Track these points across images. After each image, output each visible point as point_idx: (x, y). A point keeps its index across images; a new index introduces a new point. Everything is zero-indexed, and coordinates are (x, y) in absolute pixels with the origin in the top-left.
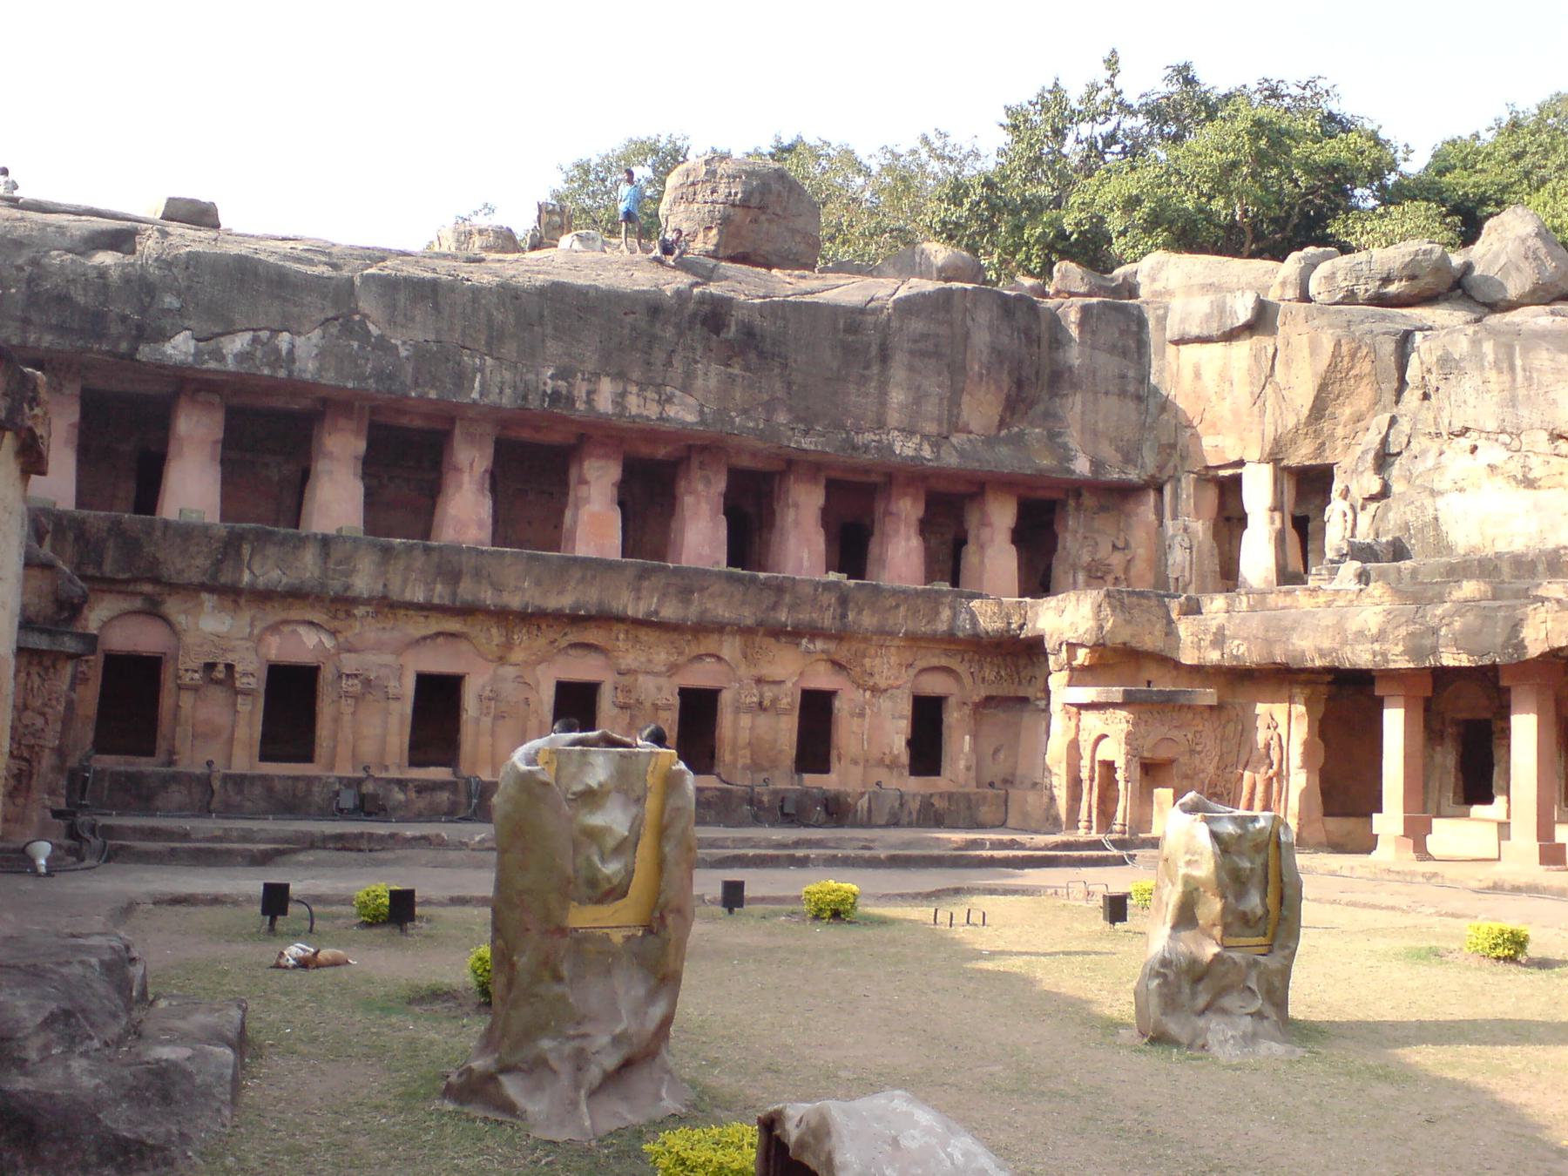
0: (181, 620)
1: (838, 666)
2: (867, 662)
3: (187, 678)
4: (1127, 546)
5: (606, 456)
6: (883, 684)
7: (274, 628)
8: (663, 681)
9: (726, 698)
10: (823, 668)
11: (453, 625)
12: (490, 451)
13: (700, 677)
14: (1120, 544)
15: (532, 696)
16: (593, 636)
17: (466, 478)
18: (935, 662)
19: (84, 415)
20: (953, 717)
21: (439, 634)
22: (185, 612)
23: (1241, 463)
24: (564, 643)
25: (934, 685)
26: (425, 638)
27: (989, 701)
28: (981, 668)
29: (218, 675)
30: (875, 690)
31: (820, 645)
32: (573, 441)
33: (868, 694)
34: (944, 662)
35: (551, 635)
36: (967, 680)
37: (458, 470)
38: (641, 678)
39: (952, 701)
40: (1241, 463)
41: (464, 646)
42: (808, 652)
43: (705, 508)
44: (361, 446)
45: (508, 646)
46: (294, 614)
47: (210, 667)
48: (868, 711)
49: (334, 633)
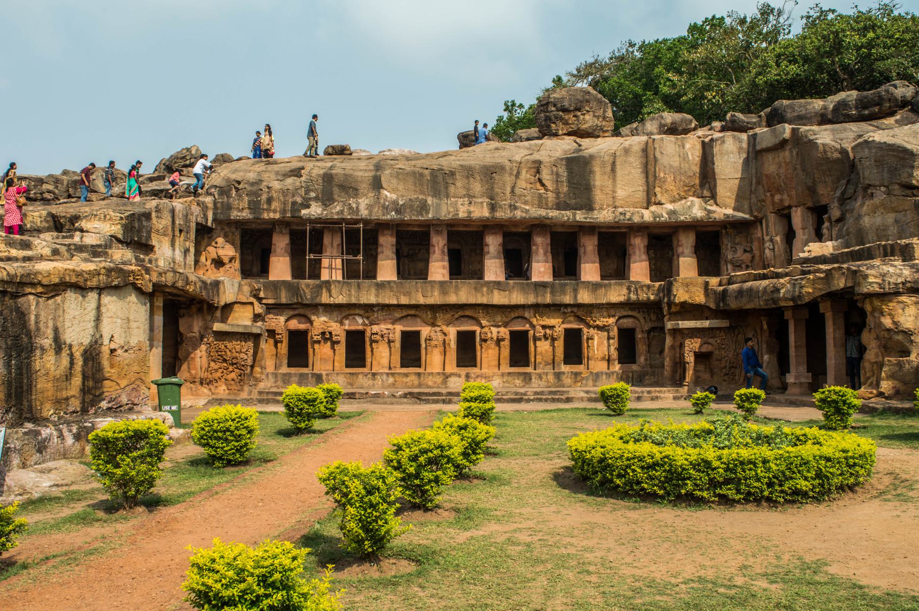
0: (313, 318)
1: (580, 320)
3: (315, 338)
4: (752, 250)
5: (495, 233)
7: (346, 317)
8: (502, 329)
10: (572, 319)
11: (412, 312)
12: (446, 237)
14: (748, 249)
15: (446, 338)
16: (468, 313)
17: (436, 248)
18: (625, 313)
19: (291, 239)
21: (408, 315)
22: (314, 314)
23: (790, 207)
24: (457, 316)
25: (627, 323)
26: (403, 317)
28: (649, 315)
29: (327, 337)
31: (569, 310)
32: (481, 229)
34: (630, 313)
35: (452, 313)
36: (642, 321)
37: (434, 246)
39: (638, 330)
40: (790, 207)
41: (418, 320)
42: (564, 313)
43: (541, 251)
44: (394, 240)
45: (435, 318)
46: (352, 312)
47: (323, 333)
48: (596, 338)
49: (368, 318)
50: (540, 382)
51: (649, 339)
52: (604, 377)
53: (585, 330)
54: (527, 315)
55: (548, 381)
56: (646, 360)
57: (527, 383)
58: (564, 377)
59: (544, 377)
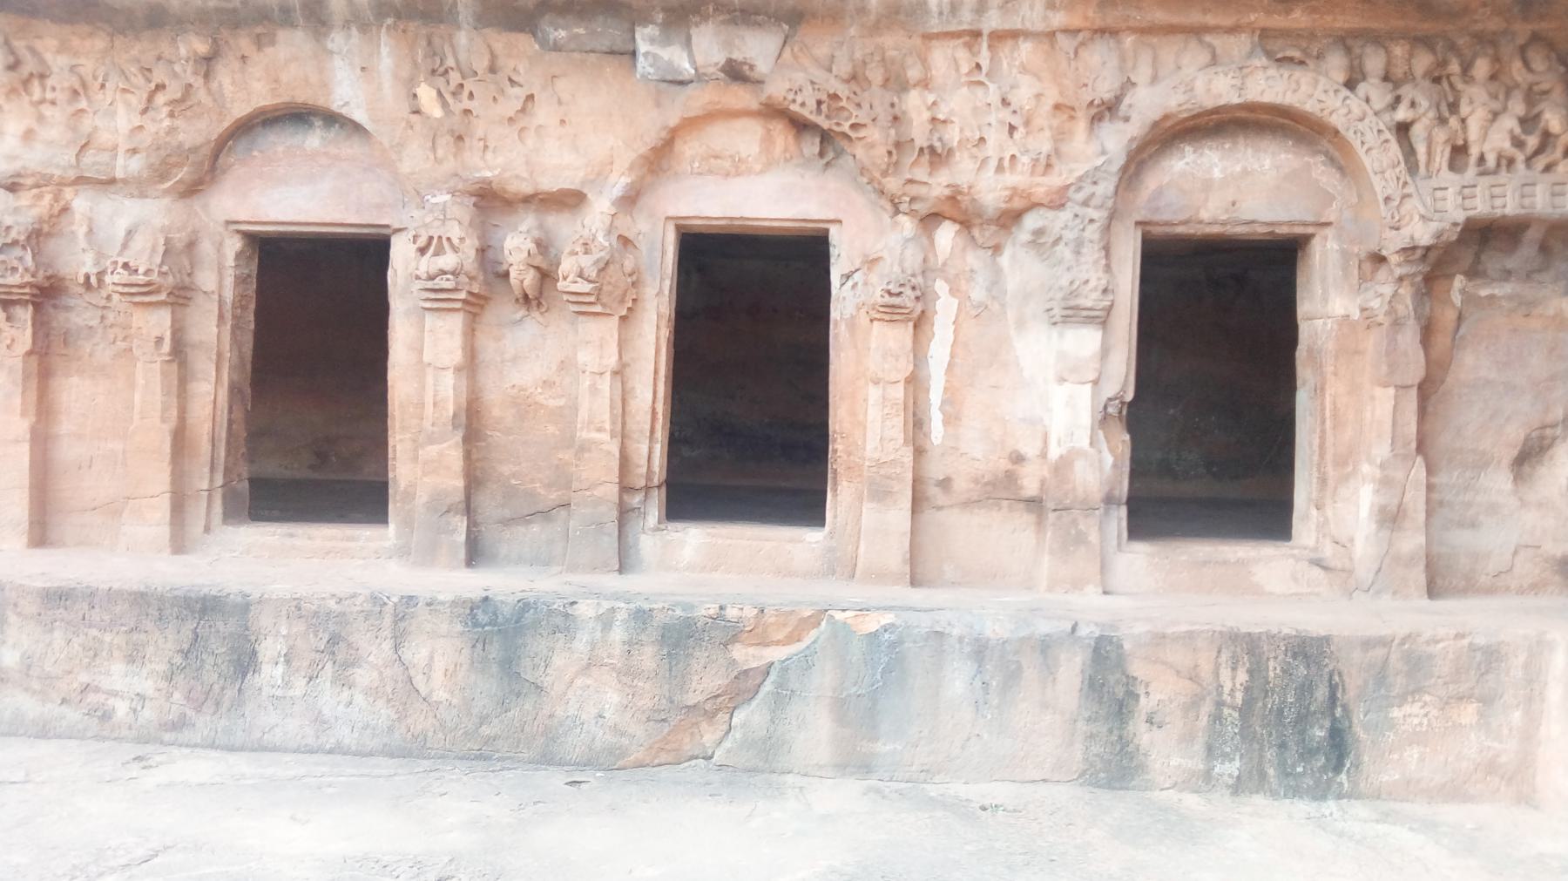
1: (815, 134)
2: (914, 103)
6: (991, 191)
9: (401, 255)
10: (745, 138)
13: (300, 194)
20: (1328, 304)
25: (1231, 190)
27: (1485, 238)
30: (957, 210)
33: (946, 235)
34: (1269, 86)
36: (1377, 155)
38: (81, 203)
48: (945, 308)
50: (329, 699)
51: (1427, 334)
52: (958, 680)
53: (867, 259)
54: (346, 91)
55: (407, 691)
56: (1391, 518)
57: (203, 700)
58: (559, 664)
59: (375, 651)
